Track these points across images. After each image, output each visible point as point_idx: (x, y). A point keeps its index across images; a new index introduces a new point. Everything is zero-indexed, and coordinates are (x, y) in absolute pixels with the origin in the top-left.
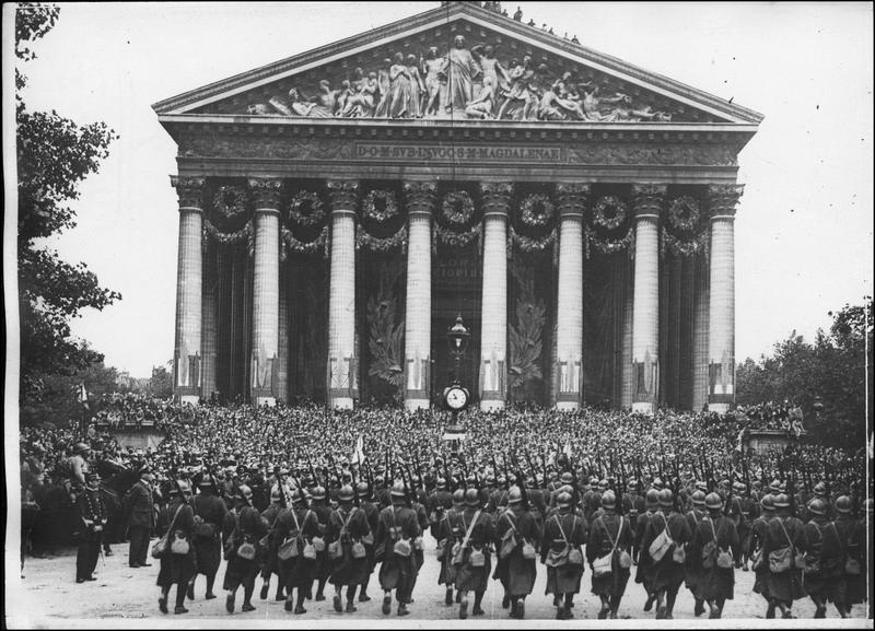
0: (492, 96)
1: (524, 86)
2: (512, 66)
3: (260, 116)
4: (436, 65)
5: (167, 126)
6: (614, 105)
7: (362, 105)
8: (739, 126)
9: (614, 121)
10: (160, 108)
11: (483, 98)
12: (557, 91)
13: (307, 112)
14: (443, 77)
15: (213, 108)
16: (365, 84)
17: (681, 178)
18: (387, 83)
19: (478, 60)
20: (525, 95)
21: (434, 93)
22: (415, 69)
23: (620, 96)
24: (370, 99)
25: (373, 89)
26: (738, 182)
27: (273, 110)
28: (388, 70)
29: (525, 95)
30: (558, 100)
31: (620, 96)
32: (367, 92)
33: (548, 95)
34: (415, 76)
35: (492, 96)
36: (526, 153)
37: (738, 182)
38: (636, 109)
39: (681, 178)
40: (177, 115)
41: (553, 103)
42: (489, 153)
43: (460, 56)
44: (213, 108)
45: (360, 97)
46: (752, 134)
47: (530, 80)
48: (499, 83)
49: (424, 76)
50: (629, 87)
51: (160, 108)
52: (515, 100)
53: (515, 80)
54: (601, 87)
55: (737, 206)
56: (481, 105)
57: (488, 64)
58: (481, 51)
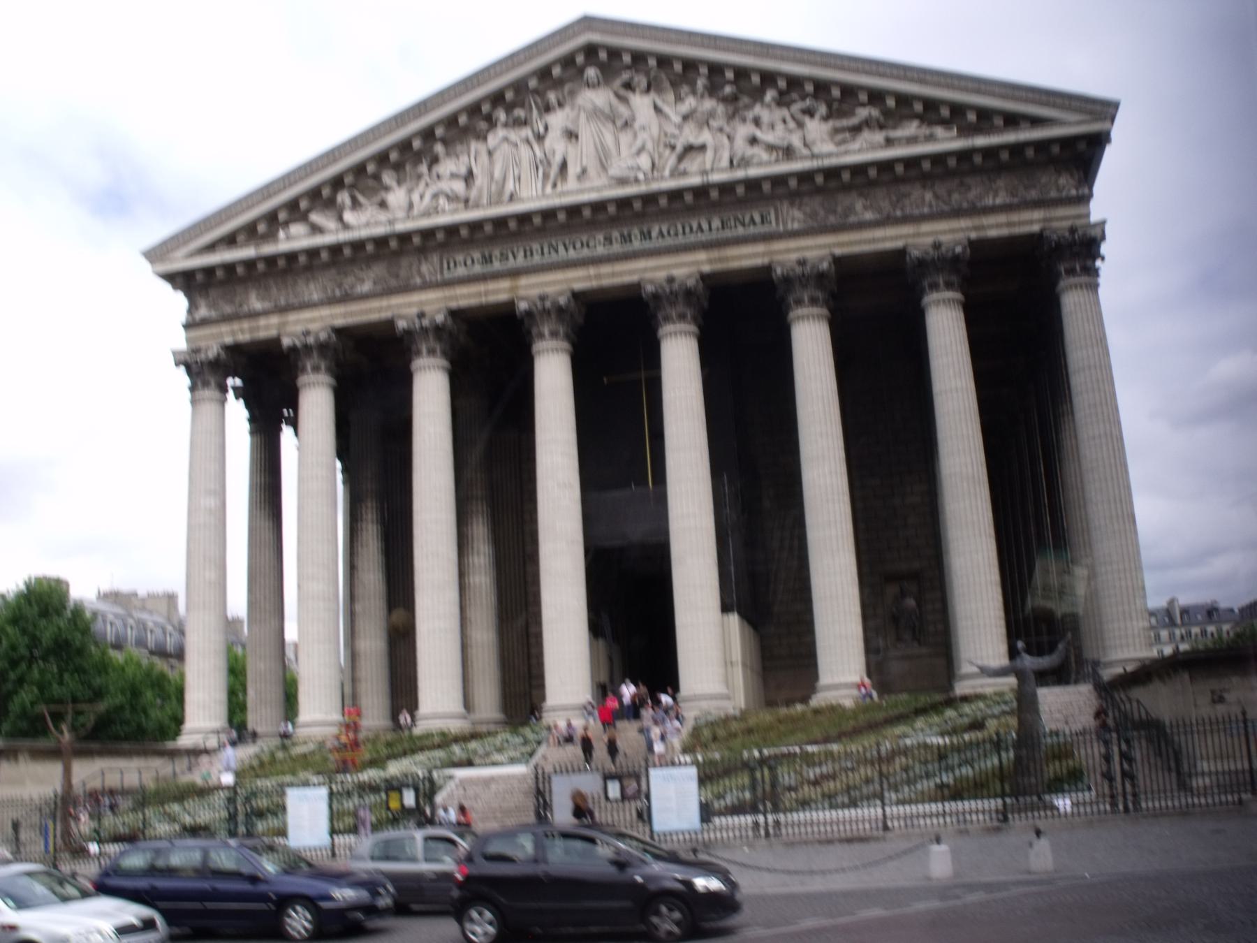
0: (649, 146)
1: (705, 123)
2: (679, 99)
3: (295, 238)
4: (558, 120)
5: (171, 278)
6: (856, 130)
7: (448, 197)
8: (1073, 126)
9: (866, 149)
10: (154, 255)
11: (634, 149)
12: (757, 122)
13: (363, 222)
14: (572, 135)
15: (230, 240)
16: (448, 166)
17: (991, 227)
18: (484, 157)
19: (623, 100)
20: (706, 137)
21: (557, 160)
22: (527, 132)
24: (459, 187)
25: (463, 171)
26: (1094, 218)
27: (316, 229)
28: (485, 139)
29: (706, 137)
30: (759, 134)
31: (863, 113)
32: (454, 176)
33: (743, 130)
34: (528, 141)
35: (649, 146)
36: (716, 223)
37: (1094, 218)
38: (895, 127)
39: (991, 227)
40: (181, 262)
41: (753, 141)
42: (654, 233)
43: (599, 98)
44: (230, 240)
45: (445, 185)
46: (1098, 141)
47: (712, 114)
48: (660, 127)
49: (540, 138)
50: (876, 97)
51: (154, 255)
52: (690, 149)
53: (686, 118)
54: (829, 106)
55: (1098, 263)
56: (630, 162)
57: (641, 104)
58: (628, 86)
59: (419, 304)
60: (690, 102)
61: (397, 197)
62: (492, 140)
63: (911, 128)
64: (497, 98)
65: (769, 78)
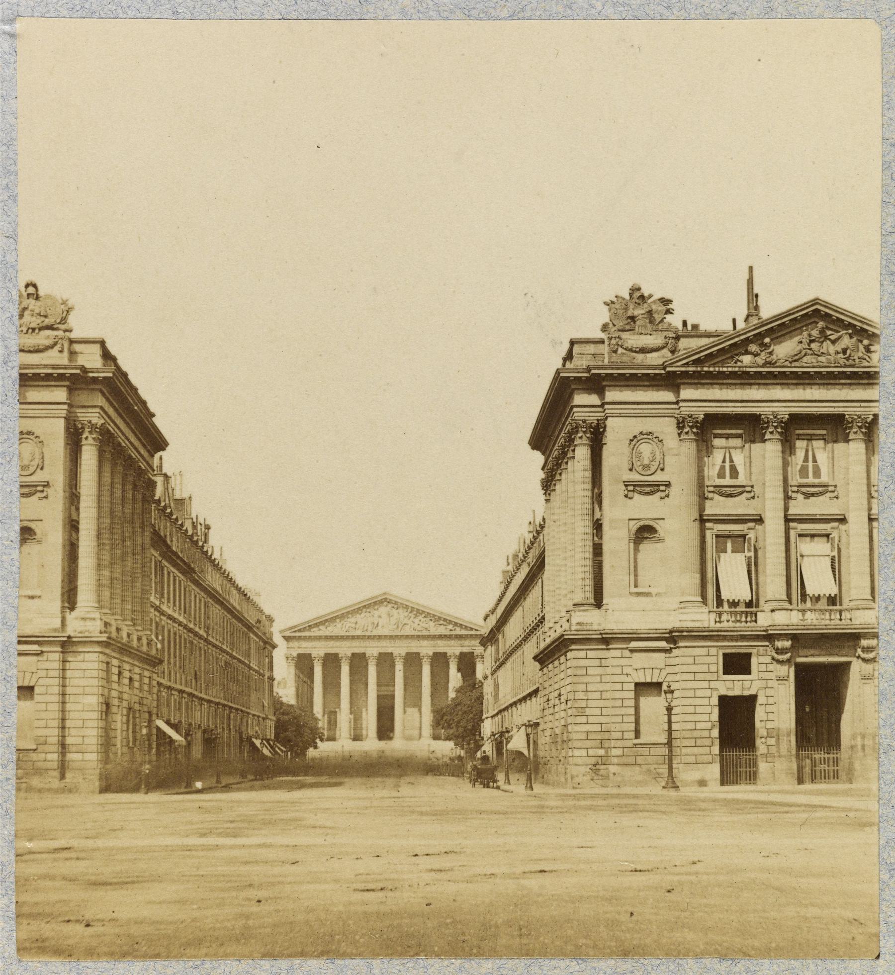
3: (315, 632)
4: (376, 613)
5: (284, 637)
15: (300, 631)
23: (442, 622)
24: (353, 625)
33: (417, 621)
40: (288, 634)
44: (300, 631)
57: (395, 611)
59: (345, 650)
60: (406, 614)
61: (339, 625)
62: (363, 615)
63: (450, 627)
64: (365, 606)
65: (423, 612)
